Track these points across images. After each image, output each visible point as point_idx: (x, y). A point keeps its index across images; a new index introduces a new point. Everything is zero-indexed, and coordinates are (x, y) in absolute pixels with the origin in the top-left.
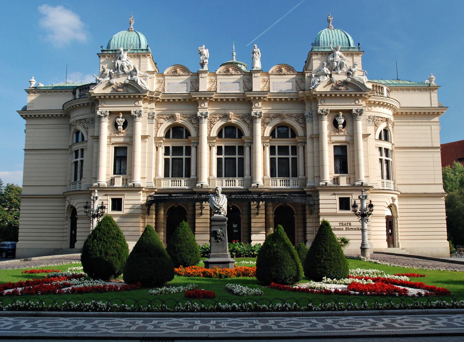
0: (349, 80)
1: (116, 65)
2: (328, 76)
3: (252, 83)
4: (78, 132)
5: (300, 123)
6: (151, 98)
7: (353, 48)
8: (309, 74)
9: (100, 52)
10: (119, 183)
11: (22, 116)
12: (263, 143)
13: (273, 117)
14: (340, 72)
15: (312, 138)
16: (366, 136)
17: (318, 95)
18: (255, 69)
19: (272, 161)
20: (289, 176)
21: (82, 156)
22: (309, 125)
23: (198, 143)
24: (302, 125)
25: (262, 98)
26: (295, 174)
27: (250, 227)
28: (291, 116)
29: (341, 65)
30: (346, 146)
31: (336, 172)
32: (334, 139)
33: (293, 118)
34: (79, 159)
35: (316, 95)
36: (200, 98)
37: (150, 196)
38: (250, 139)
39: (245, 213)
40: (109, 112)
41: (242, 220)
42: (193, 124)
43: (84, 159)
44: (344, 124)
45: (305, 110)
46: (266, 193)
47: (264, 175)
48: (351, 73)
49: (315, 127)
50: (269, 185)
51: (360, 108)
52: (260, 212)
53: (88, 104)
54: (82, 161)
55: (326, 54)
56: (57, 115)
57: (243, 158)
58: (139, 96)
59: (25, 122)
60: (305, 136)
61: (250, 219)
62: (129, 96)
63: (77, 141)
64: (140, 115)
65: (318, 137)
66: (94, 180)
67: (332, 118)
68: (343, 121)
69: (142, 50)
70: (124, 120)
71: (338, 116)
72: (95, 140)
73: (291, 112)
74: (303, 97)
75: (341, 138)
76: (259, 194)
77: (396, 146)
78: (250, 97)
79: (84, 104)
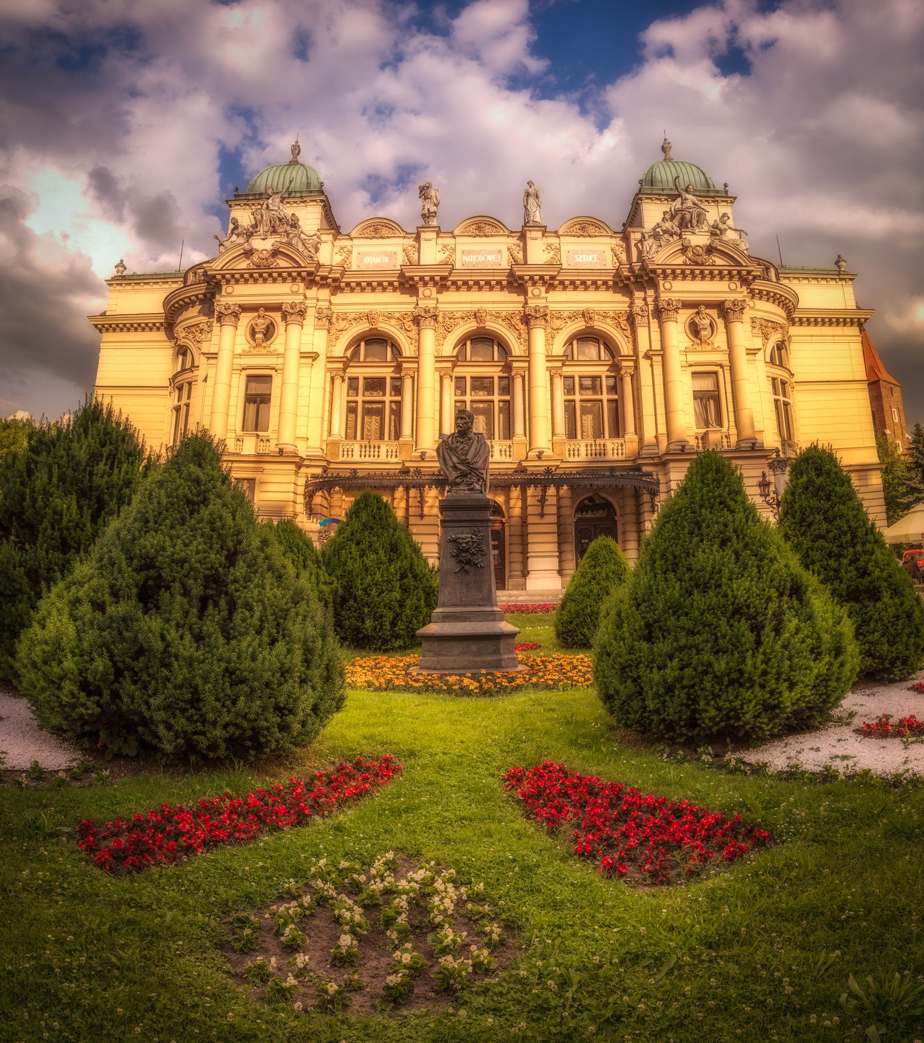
0: (717, 244)
7: (717, 191)
12: (549, 369)
14: (697, 230)
16: (752, 352)
18: (531, 224)
22: (642, 333)
29: (701, 218)
30: (716, 373)
32: (693, 358)
33: (608, 320)
40: (240, 306)
51: (739, 297)
58: (299, 274)
64: (302, 313)
67: (684, 316)
68: (707, 322)
70: (268, 322)
72: (211, 361)
74: (628, 278)
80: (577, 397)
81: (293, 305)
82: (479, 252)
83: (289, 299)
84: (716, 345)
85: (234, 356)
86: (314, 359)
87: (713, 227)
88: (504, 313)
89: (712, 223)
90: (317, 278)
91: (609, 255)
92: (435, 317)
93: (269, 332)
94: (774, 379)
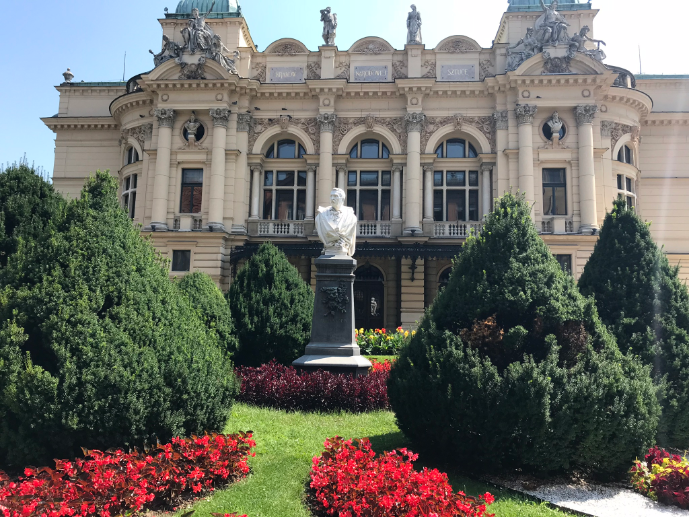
1: (187, 35)
2: (535, 50)
3: (407, 67)
4: (130, 150)
5: (485, 133)
6: (242, 88)
8: (503, 51)
9: (164, 17)
10: (186, 223)
11: (49, 126)
12: (422, 165)
13: (441, 123)
15: (506, 156)
17: (519, 82)
19: (438, 194)
20: (464, 220)
21: (135, 187)
22: (500, 135)
23: (317, 165)
24: (488, 135)
25: (423, 89)
26: (474, 216)
27: (398, 301)
28: (470, 121)
30: (564, 169)
31: (546, 213)
34: (130, 190)
35: (516, 81)
36: (322, 90)
37: (237, 248)
38: (402, 159)
39: (392, 276)
40: (174, 111)
41: (385, 289)
42: (309, 134)
43: (138, 190)
44: (563, 130)
45: (494, 108)
46: (426, 245)
47: (424, 217)
48: (577, 44)
49: (512, 138)
50: (430, 232)
51: (590, 102)
52: (416, 276)
53: (144, 102)
54: (134, 194)
55: (532, 17)
56: (103, 126)
57: (389, 191)
58: (222, 85)
59: (54, 136)
60: (494, 152)
61: (399, 287)
62: (206, 85)
63: (129, 162)
65: (514, 154)
66: (147, 221)
67: (539, 122)
69: (231, 14)
70: (197, 125)
71: (551, 118)
73: (471, 114)
74: (493, 87)
75: (555, 157)
76: (417, 245)
77: (643, 174)
78: (403, 88)
79: (137, 103)
80: (445, 188)
81: (218, 112)
82: (369, 68)
83: (216, 106)
84: (566, 144)
85: (172, 153)
86: (237, 155)
87: (573, 40)
88: (388, 119)
89: (571, 36)
90: (238, 89)
91: (477, 69)
92: (332, 123)
93: (200, 134)
94: (619, 177)
